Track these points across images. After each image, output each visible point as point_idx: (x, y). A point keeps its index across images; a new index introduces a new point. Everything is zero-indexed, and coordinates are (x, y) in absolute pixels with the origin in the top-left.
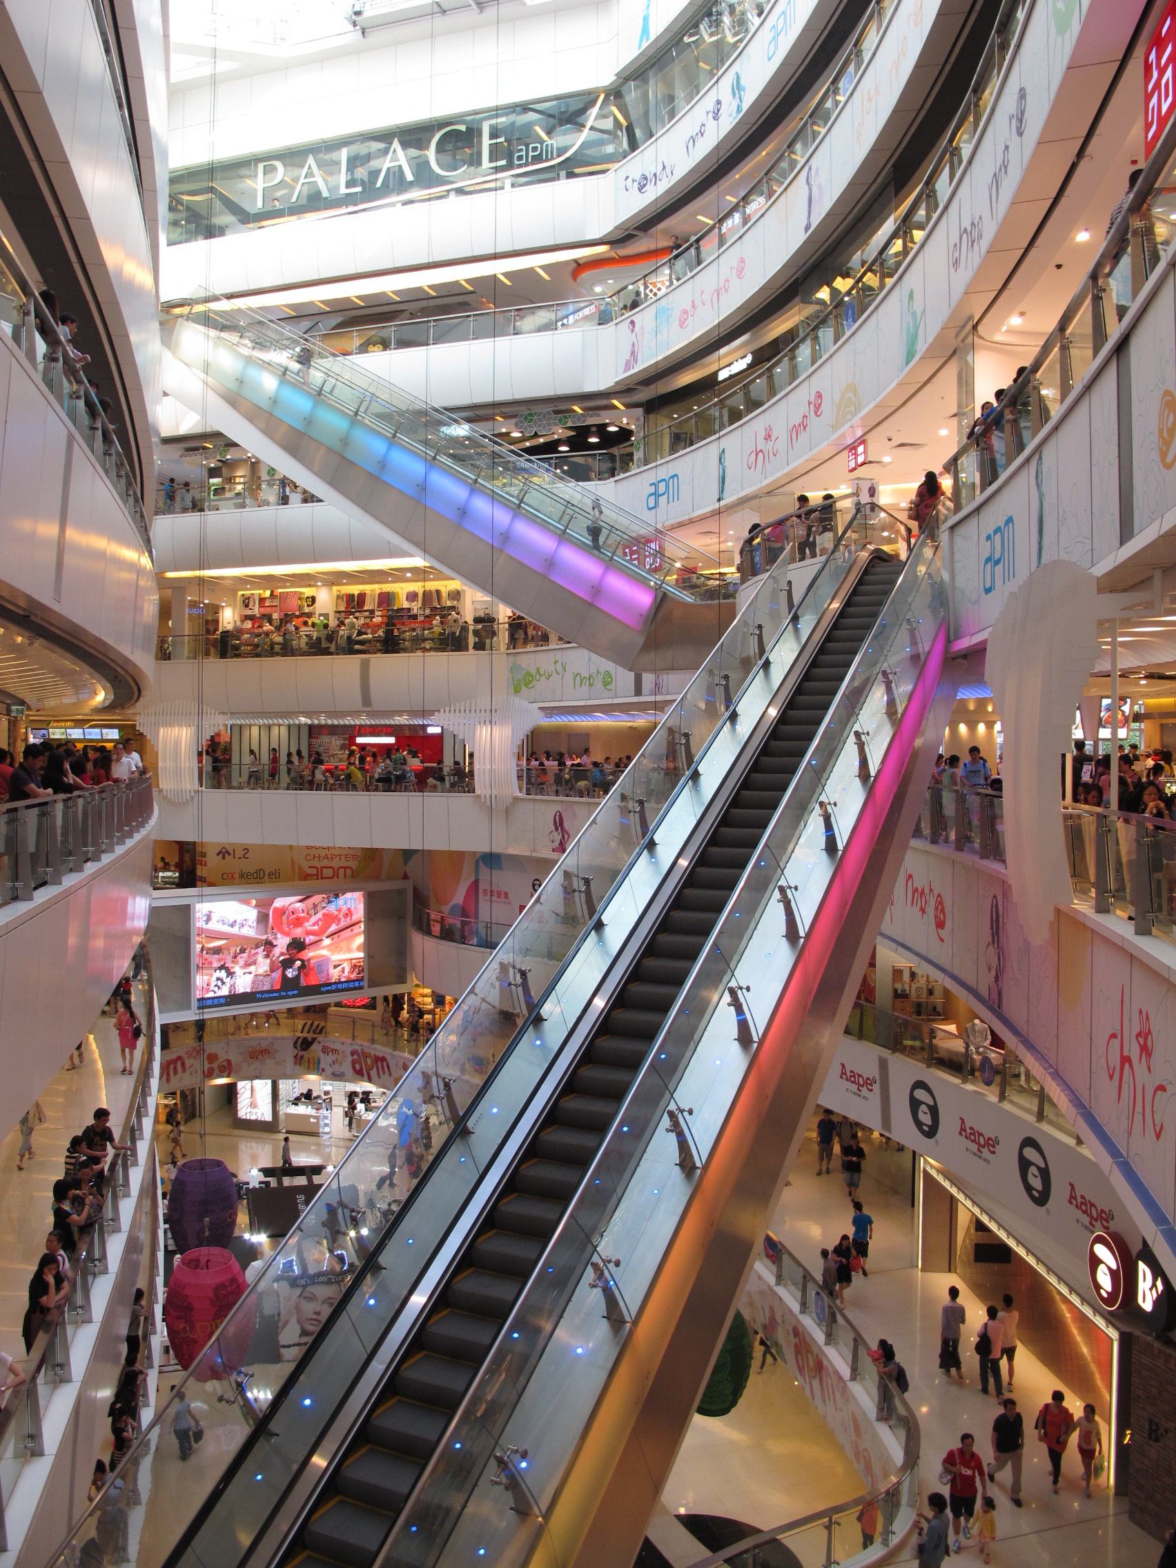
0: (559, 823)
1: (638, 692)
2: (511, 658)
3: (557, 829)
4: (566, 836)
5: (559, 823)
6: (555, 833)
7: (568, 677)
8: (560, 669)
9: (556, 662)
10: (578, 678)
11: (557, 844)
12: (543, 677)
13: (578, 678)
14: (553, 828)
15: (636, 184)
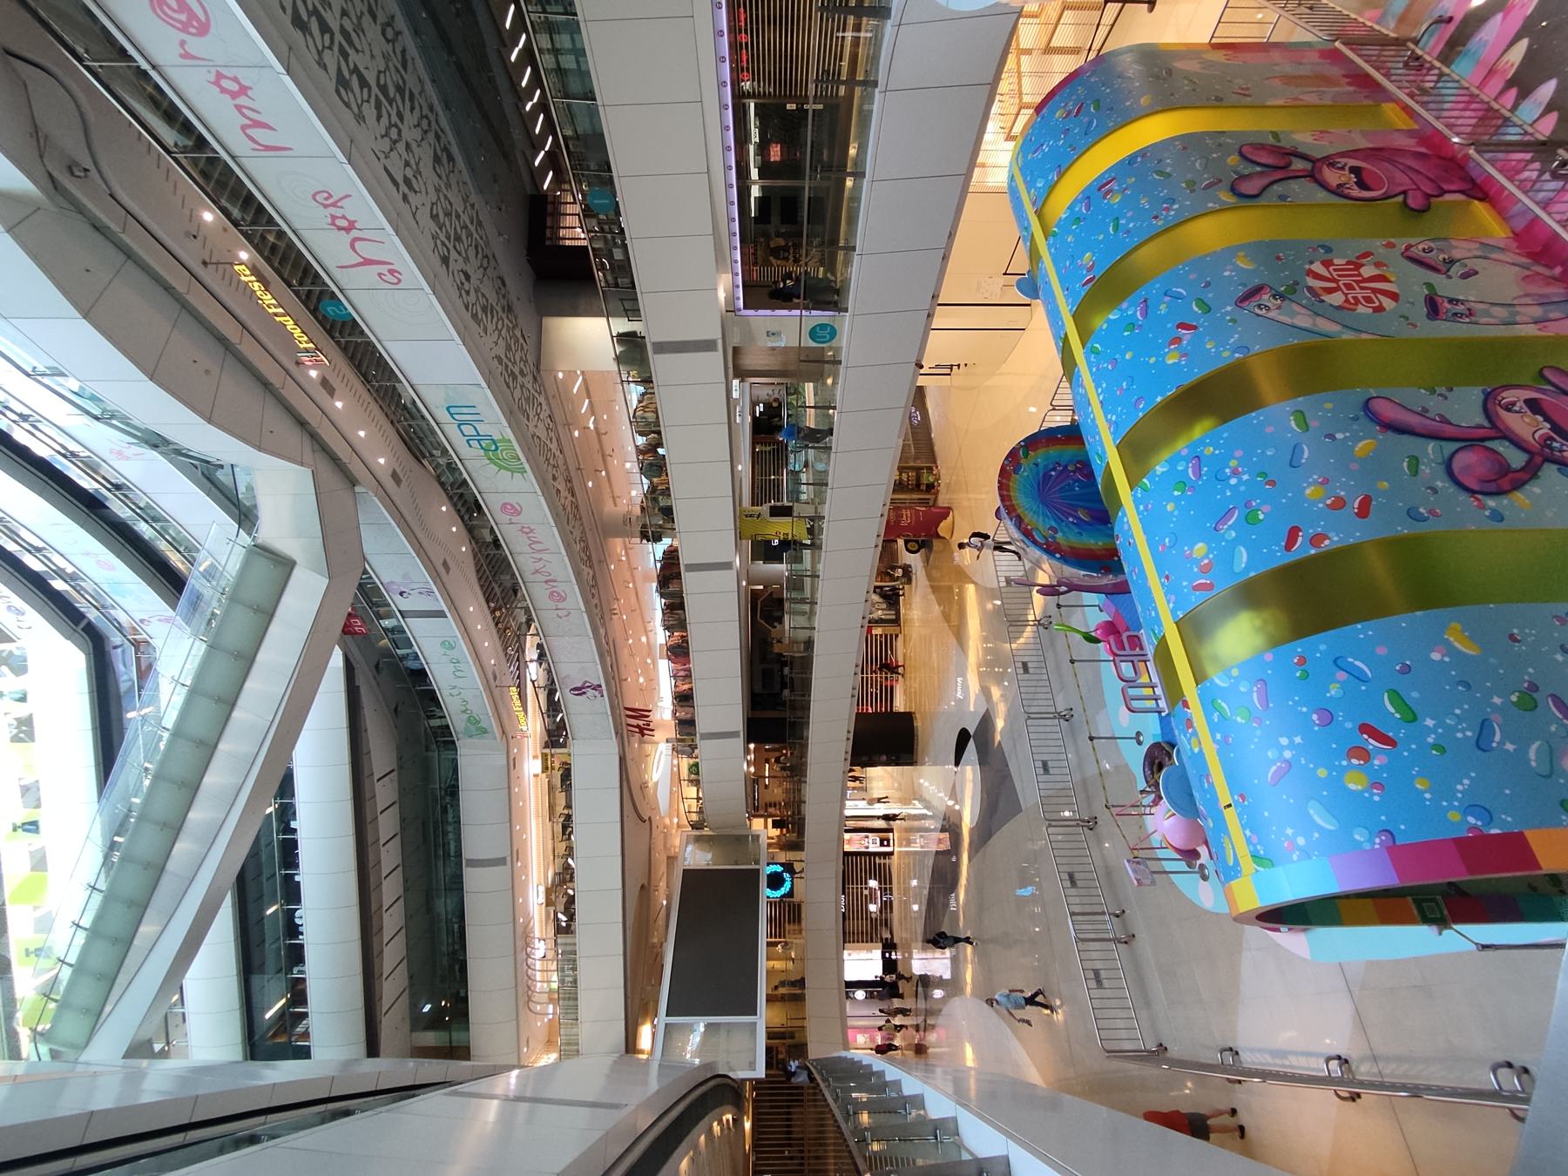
0: (579, 691)
1: (440, 614)
2: (460, 736)
3: (584, 693)
4: (588, 684)
5: (579, 691)
6: (588, 694)
7: (460, 683)
8: (455, 692)
9: (451, 695)
10: (461, 674)
11: (597, 693)
12: (468, 706)
13: (461, 674)
14: (584, 696)
15: (20, 618)
